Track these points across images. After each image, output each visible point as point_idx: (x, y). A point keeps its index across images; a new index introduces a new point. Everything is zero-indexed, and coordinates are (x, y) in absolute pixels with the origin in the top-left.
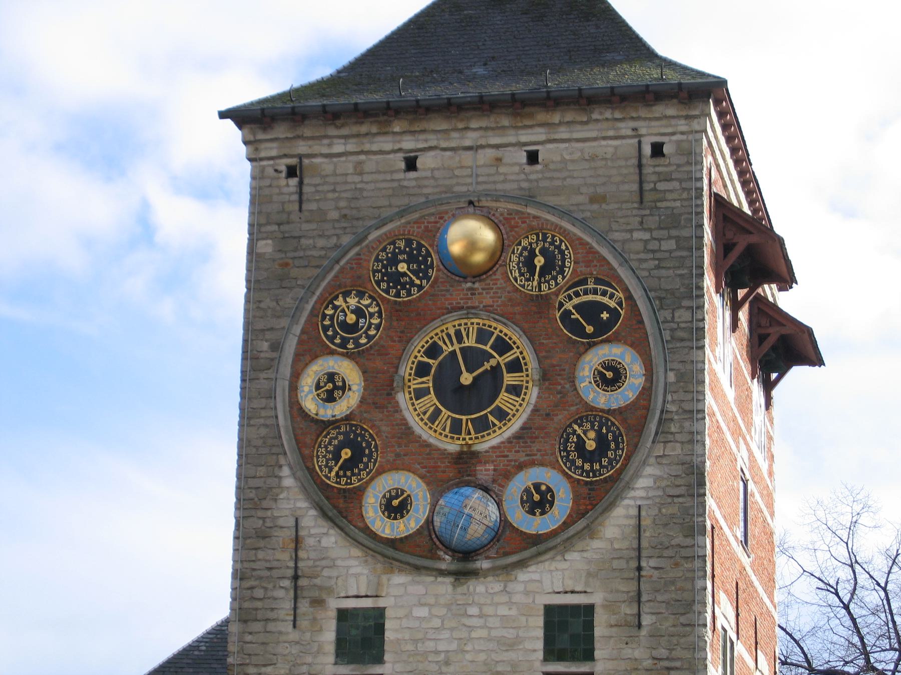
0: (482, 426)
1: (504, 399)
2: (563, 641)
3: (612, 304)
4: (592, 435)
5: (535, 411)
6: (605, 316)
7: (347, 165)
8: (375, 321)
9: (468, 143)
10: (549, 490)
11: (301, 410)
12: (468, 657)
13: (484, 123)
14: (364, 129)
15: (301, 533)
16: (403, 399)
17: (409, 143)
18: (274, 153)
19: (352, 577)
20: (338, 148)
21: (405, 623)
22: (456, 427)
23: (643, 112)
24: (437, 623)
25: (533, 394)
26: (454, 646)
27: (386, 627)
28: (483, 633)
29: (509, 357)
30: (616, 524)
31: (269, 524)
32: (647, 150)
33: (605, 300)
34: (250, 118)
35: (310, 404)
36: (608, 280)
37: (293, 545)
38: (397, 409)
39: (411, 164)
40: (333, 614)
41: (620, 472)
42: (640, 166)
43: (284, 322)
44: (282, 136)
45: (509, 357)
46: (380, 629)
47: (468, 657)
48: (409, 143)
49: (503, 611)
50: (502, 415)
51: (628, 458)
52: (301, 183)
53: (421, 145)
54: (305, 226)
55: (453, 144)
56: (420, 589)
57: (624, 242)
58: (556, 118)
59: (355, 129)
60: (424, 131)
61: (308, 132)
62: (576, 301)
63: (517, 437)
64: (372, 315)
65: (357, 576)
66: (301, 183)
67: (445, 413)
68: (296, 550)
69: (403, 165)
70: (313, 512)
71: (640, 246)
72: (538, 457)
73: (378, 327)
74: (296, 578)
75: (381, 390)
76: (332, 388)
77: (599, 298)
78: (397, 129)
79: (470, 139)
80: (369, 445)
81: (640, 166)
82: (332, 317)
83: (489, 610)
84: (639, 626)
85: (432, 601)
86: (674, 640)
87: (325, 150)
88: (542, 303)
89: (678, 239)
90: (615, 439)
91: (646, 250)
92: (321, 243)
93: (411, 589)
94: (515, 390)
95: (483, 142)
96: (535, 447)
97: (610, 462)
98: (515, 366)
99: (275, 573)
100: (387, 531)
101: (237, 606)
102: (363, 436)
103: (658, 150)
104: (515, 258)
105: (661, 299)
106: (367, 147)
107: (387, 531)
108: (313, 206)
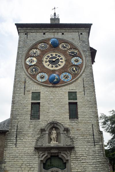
0: (56, 67)
1: (60, 63)
2: (71, 97)
3: (76, 52)
4: (74, 68)
5: (65, 64)
6: (75, 53)
7: (34, 34)
8: (39, 53)
9: (53, 31)
10: (68, 75)
11: (27, 64)
12: (55, 99)
13: (56, 29)
14: (37, 29)
15: (26, 81)
16: (44, 63)
17: (44, 31)
18: (23, 31)
19: (34, 87)
20: (34, 31)
21: (44, 94)
22: (52, 67)
23: (79, 29)
24: (50, 94)
25: (64, 62)
26: (52, 98)
27: (41, 95)
28: (58, 96)
29: (60, 58)
30: (80, 81)
31: (20, 79)
32: (80, 34)
33: (75, 51)
34: (20, 27)
35: (28, 63)
36: (76, 49)
37: (24, 83)
38: (42, 64)
39: (44, 34)
40: (31, 93)
41: (79, 73)
42: (79, 35)
43: (24, 52)
44: (25, 29)
45: (60, 58)
46: (39, 95)
47: (55, 99)
48: (44, 31)
49: (61, 92)
50: (60, 65)
51: (80, 71)
52: (27, 35)
53: (46, 31)
54: (28, 41)
55: (51, 31)
56: (47, 89)
57: (78, 44)
58: (66, 29)
59: (36, 29)
60: (46, 30)
61: (28, 29)
62: (70, 51)
63: (62, 68)
64: (38, 52)
65: (36, 87)
66: (27, 35)
67: (50, 65)
68: (25, 83)
69: (43, 34)
70: (28, 78)
71: (80, 45)
72: (66, 71)
73: (39, 53)
74: (25, 87)
75: (40, 61)
76: (32, 61)
77: (74, 51)
78: (42, 29)
79: (54, 31)
80: (38, 69)
81: (79, 35)
82: (32, 52)
83: (58, 92)
84: (85, 95)
85: (49, 91)
86: (91, 97)
87: (31, 31)
88: (65, 51)
89: (85, 44)
90: (78, 69)
91: (81, 45)
92: (30, 43)
93: (45, 89)
94: (62, 62)
95: (55, 31)
96: (65, 69)
97: (77, 72)
98: (61, 59)
99: (21, 87)
100: (41, 81)
101: (14, 91)
102: (37, 68)
103: (81, 34)
104: (61, 46)
105: (84, 51)
106: (38, 31)
107: (41, 81)
108: (29, 38)
